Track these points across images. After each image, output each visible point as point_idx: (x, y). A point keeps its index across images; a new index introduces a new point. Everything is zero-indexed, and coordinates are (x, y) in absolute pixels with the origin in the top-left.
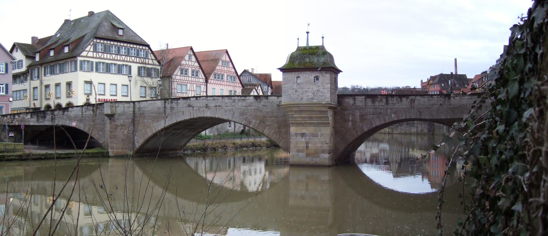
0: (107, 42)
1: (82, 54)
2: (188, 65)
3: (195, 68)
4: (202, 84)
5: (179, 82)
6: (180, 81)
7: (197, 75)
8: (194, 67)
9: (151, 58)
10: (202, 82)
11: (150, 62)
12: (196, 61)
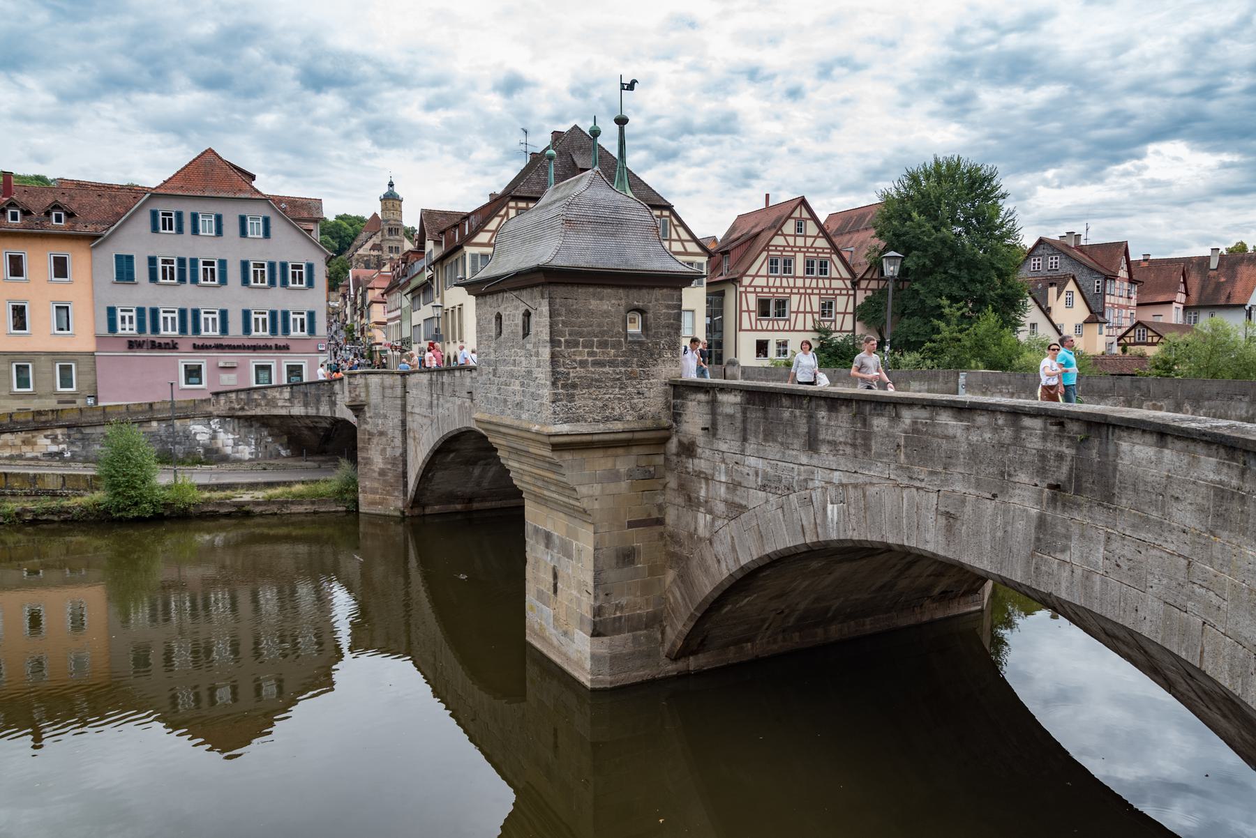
0: (527, 205)
1: (476, 240)
2: (795, 246)
3: (815, 252)
4: (841, 294)
5: (762, 292)
6: (766, 290)
7: (823, 271)
9: (677, 238)
10: (841, 289)
11: (677, 247)
12: (821, 235)
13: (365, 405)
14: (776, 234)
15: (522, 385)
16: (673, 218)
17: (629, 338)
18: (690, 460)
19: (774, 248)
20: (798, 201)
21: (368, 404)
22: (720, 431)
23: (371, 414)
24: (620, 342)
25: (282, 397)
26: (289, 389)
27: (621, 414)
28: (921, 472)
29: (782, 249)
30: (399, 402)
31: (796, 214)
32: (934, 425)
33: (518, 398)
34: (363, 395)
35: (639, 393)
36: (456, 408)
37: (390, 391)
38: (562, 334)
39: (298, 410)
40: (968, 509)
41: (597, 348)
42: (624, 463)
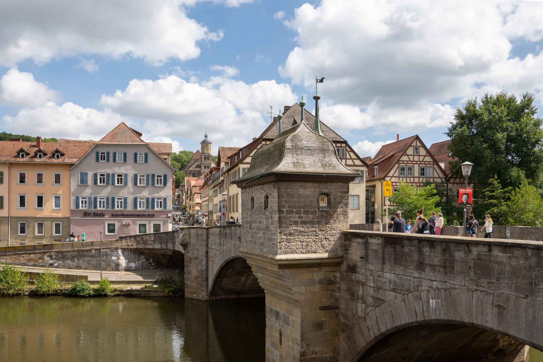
8: (424, 163)
12: (427, 155)
13: (188, 244)
14: (403, 155)
15: (264, 234)
16: (347, 148)
17: (321, 209)
18: (354, 275)
19: (402, 162)
20: (415, 137)
21: (190, 244)
22: (370, 259)
23: (191, 249)
24: (315, 211)
25: (150, 239)
26: (153, 236)
27: (316, 249)
28: (484, 282)
29: (406, 162)
30: (205, 242)
31: (414, 144)
32: (490, 256)
33: (261, 241)
34: (187, 239)
35: (326, 238)
36: (233, 246)
37: (201, 237)
38: (285, 207)
39: (157, 246)
40: (511, 303)
41: (303, 214)
42: (318, 275)
